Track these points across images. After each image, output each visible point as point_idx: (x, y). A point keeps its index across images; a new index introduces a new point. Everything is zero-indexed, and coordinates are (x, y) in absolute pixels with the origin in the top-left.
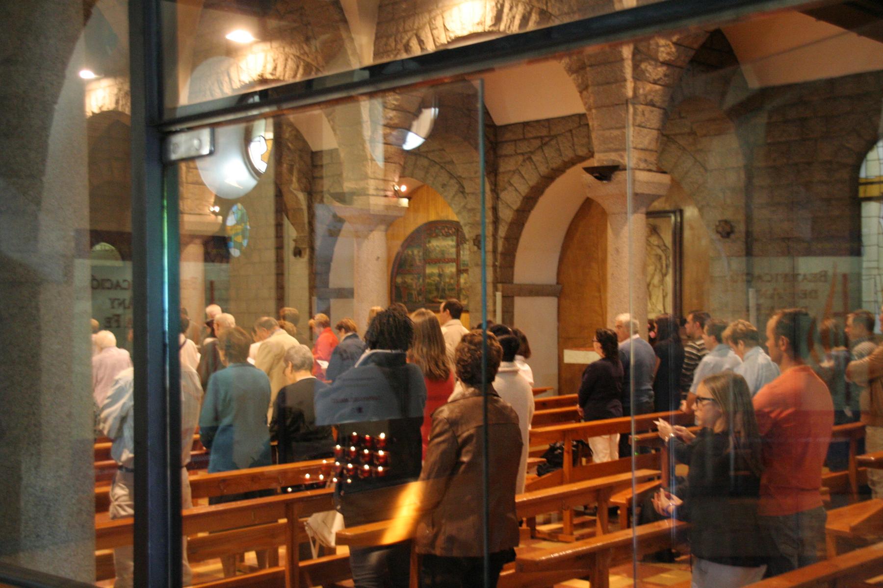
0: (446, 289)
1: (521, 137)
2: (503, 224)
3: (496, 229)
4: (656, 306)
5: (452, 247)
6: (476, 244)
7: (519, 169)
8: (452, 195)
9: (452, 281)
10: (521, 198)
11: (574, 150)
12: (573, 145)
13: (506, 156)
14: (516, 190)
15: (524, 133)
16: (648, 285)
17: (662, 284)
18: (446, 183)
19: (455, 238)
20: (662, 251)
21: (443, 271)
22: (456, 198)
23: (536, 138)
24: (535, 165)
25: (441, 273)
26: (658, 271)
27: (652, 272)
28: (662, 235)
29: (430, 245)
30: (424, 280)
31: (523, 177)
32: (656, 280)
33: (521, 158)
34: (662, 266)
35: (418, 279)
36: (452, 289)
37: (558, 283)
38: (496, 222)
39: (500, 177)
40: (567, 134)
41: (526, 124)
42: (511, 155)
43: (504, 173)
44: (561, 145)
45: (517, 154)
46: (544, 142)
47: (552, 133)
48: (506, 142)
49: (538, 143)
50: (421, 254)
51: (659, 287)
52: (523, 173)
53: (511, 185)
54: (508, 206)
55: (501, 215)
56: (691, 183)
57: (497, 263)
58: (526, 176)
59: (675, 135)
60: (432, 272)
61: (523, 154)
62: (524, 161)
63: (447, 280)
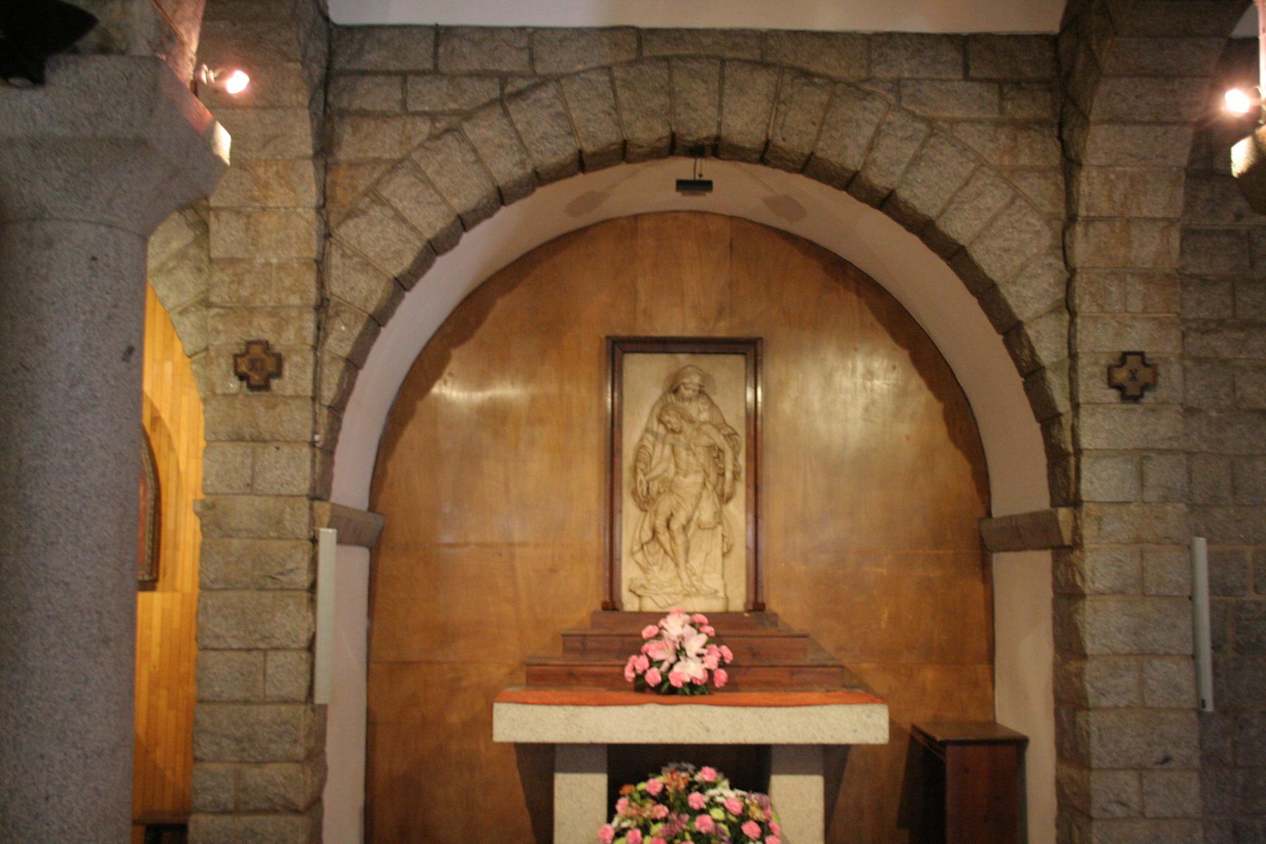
1: (428, 65)
2: (346, 316)
3: (321, 329)
4: (701, 580)
7: (415, 156)
10: (419, 244)
11: (619, 123)
12: (617, 108)
13: (364, 114)
14: (400, 218)
15: (435, 56)
16: (685, 528)
17: (720, 523)
20: (724, 435)
23: (482, 75)
24: (474, 150)
26: (709, 486)
27: (695, 490)
28: (715, 399)
31: (429, 183)
32: (706, 513)
33: (424, 127)
34: (723, 475)
37: (372, 508)
38: (323, 307)
39: (342, 176)
40: (593, 76)
41: (440, 34)
42: (384, 116)
43: (353, 165)
44: (572, 105)
45: (405, 110)
46: (510, 89)
47: (540, 69)
48: (364, 73)
49: (489, 90)
51: (713, 528)
52: (429, 172)
53: (384, 203)
54: (366, 265)
55: (335, 287)
56: (1006, 250)
57: (317, 438)
58: (442, 183)
59: (954, 122)
61: (432, 116)
62: (434, 137)
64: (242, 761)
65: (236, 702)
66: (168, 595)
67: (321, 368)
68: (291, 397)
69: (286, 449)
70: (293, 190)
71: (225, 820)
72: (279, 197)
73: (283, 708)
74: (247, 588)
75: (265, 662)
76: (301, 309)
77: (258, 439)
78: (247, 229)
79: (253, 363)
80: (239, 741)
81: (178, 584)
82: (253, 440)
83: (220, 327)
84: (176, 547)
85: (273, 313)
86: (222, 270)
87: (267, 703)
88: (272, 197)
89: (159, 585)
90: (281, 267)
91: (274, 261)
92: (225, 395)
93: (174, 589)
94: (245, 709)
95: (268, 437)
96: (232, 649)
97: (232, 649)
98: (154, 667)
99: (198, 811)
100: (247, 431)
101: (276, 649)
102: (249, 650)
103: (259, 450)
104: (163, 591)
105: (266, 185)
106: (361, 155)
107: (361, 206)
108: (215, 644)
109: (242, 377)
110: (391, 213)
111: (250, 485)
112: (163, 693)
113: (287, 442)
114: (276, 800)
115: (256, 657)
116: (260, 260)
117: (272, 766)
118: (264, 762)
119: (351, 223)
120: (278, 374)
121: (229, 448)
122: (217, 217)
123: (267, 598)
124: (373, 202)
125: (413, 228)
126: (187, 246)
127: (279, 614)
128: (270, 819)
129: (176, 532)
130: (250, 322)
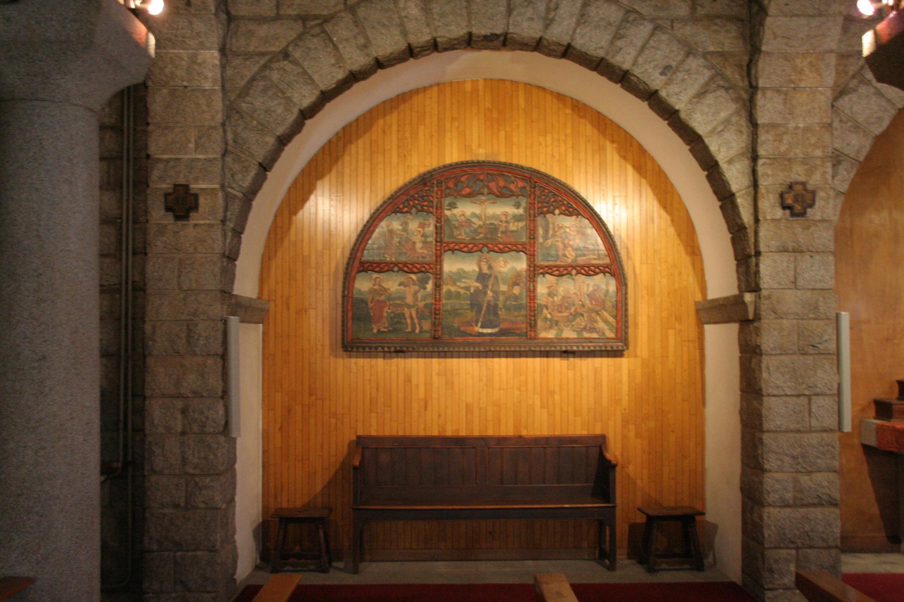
0: (500, 304)
5: (517, 219)
6: (789, 201)
8: (692, 90)
9: (516, 290)
10: (893, 112)
18: (674, 64)
19: (524, 202)
21: (490, 267)
22: (709, 99)
25: (485, 270)
29: (455, 211)
30: (438, 286)
35: (423, 283)
36: (518, 308)
50: (431, 229)
60: (462, 270)
63: (504, 288)
64: (797, 472)
65: (791, 431)
66: (632, 360)
67: (486, 200)
68: (820, 221)
69: (817, 257)
70: (820, 75)
71: (788, 511)
72: (809, 79)
73: (825, 435)
74: (794, 354)
75: (810, 403)
76: (823, 159)
77: (797, 251)
78: (785, 103)
79: (796, 199)
80: (794, 458)
81: (639, 353)
82: (794, 251)
83: (769, 172)
84: (636, 325)
85: (804, 162)
86: (768, 132)
87: (813, 432)
88: (804, 80)
89: (626, 353)
90: (807, 130)
91: (801, 125)
92: (773, 220)
93: (636, 356)
94: (798, 436)
95: (804, 248)
96: (787, 395)
97: (787, 395)
98: (625, 410)
99: (770, 505)
100: (790, 245)
101: (817, 395)
102: (798, 396)
103: (799, 258)
104: (628, 357)
105: (801, 71)
106: (849, 49)
107: (851, 85)
108: (775, 392)
109: (784, 207)
110: (872, 90)
111: (794, 282)
112: (632, 427)
113: (818, 252)
114: (824, 497)
115: (803, 401)
116: (792, 125)
117: (819, 474)
118: (811, 472)
119: (846, 98)
120: (811, 206)
121: (777, 256)
122: (764, 94)
123: (810, 360)
124: (860, 82)
125: (889, 101)
126: (732, 115)
127: (819, 371)
128: (818, 510)
129: (635, 316)
130: (791, 169)
